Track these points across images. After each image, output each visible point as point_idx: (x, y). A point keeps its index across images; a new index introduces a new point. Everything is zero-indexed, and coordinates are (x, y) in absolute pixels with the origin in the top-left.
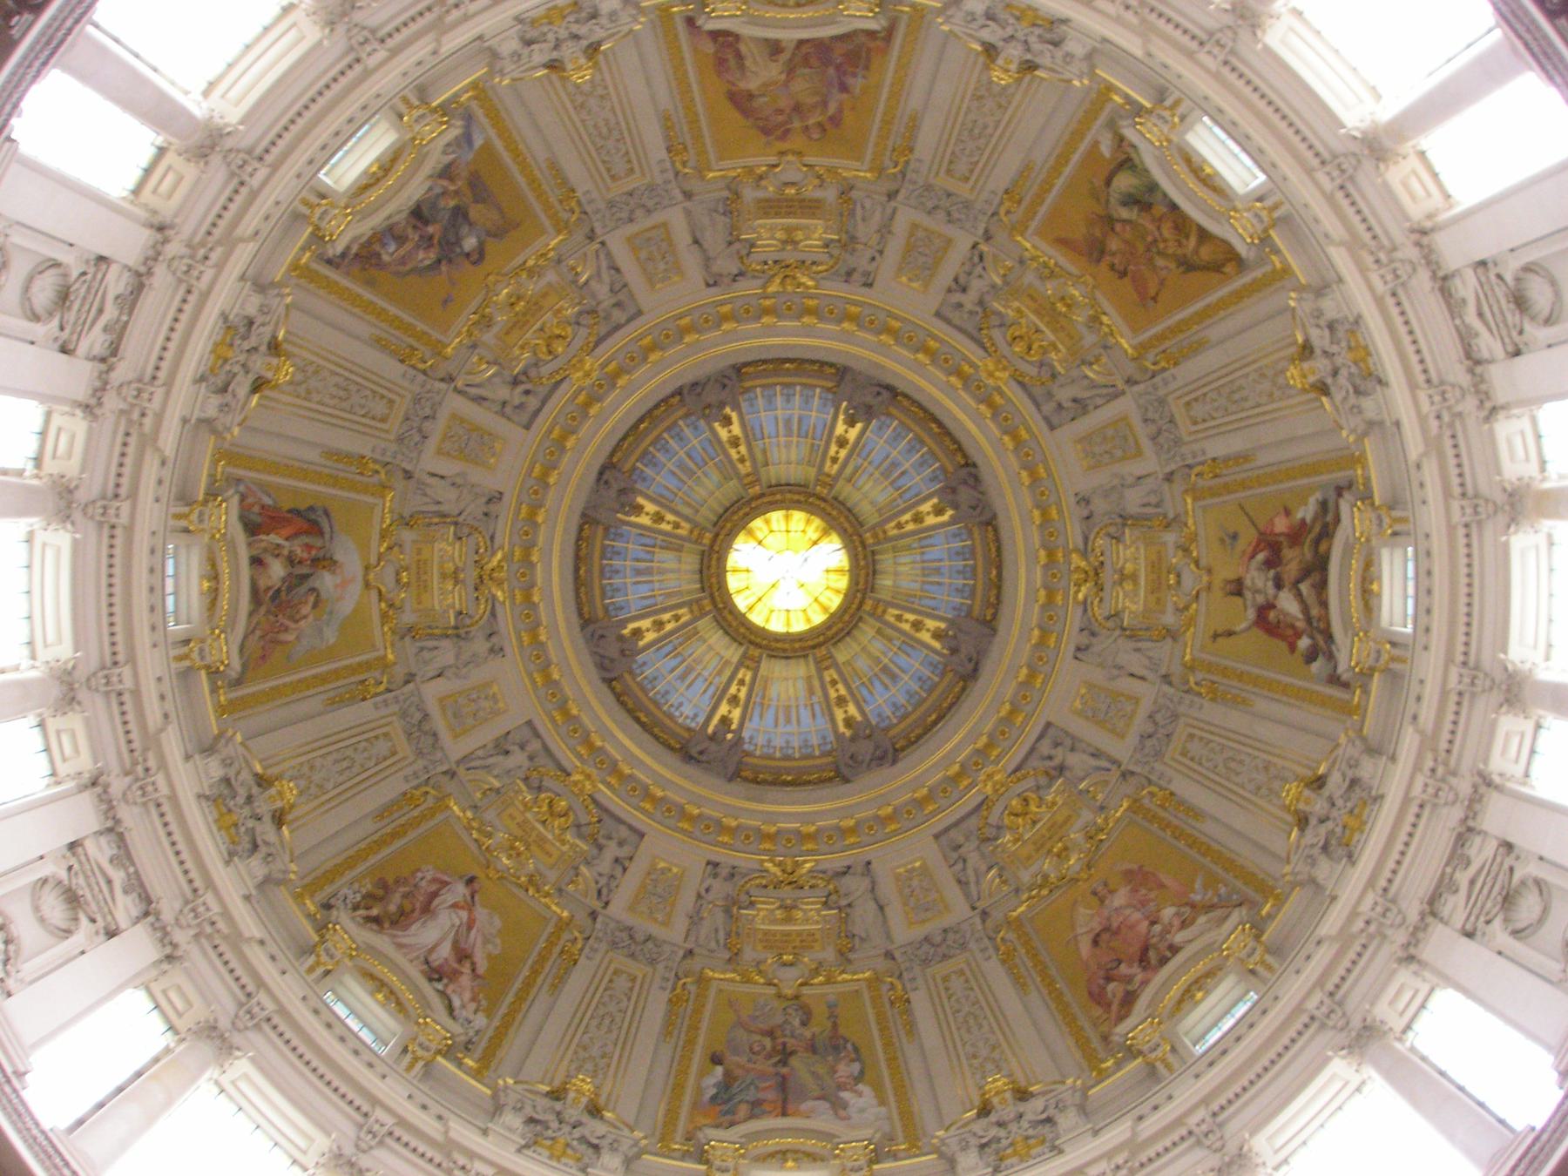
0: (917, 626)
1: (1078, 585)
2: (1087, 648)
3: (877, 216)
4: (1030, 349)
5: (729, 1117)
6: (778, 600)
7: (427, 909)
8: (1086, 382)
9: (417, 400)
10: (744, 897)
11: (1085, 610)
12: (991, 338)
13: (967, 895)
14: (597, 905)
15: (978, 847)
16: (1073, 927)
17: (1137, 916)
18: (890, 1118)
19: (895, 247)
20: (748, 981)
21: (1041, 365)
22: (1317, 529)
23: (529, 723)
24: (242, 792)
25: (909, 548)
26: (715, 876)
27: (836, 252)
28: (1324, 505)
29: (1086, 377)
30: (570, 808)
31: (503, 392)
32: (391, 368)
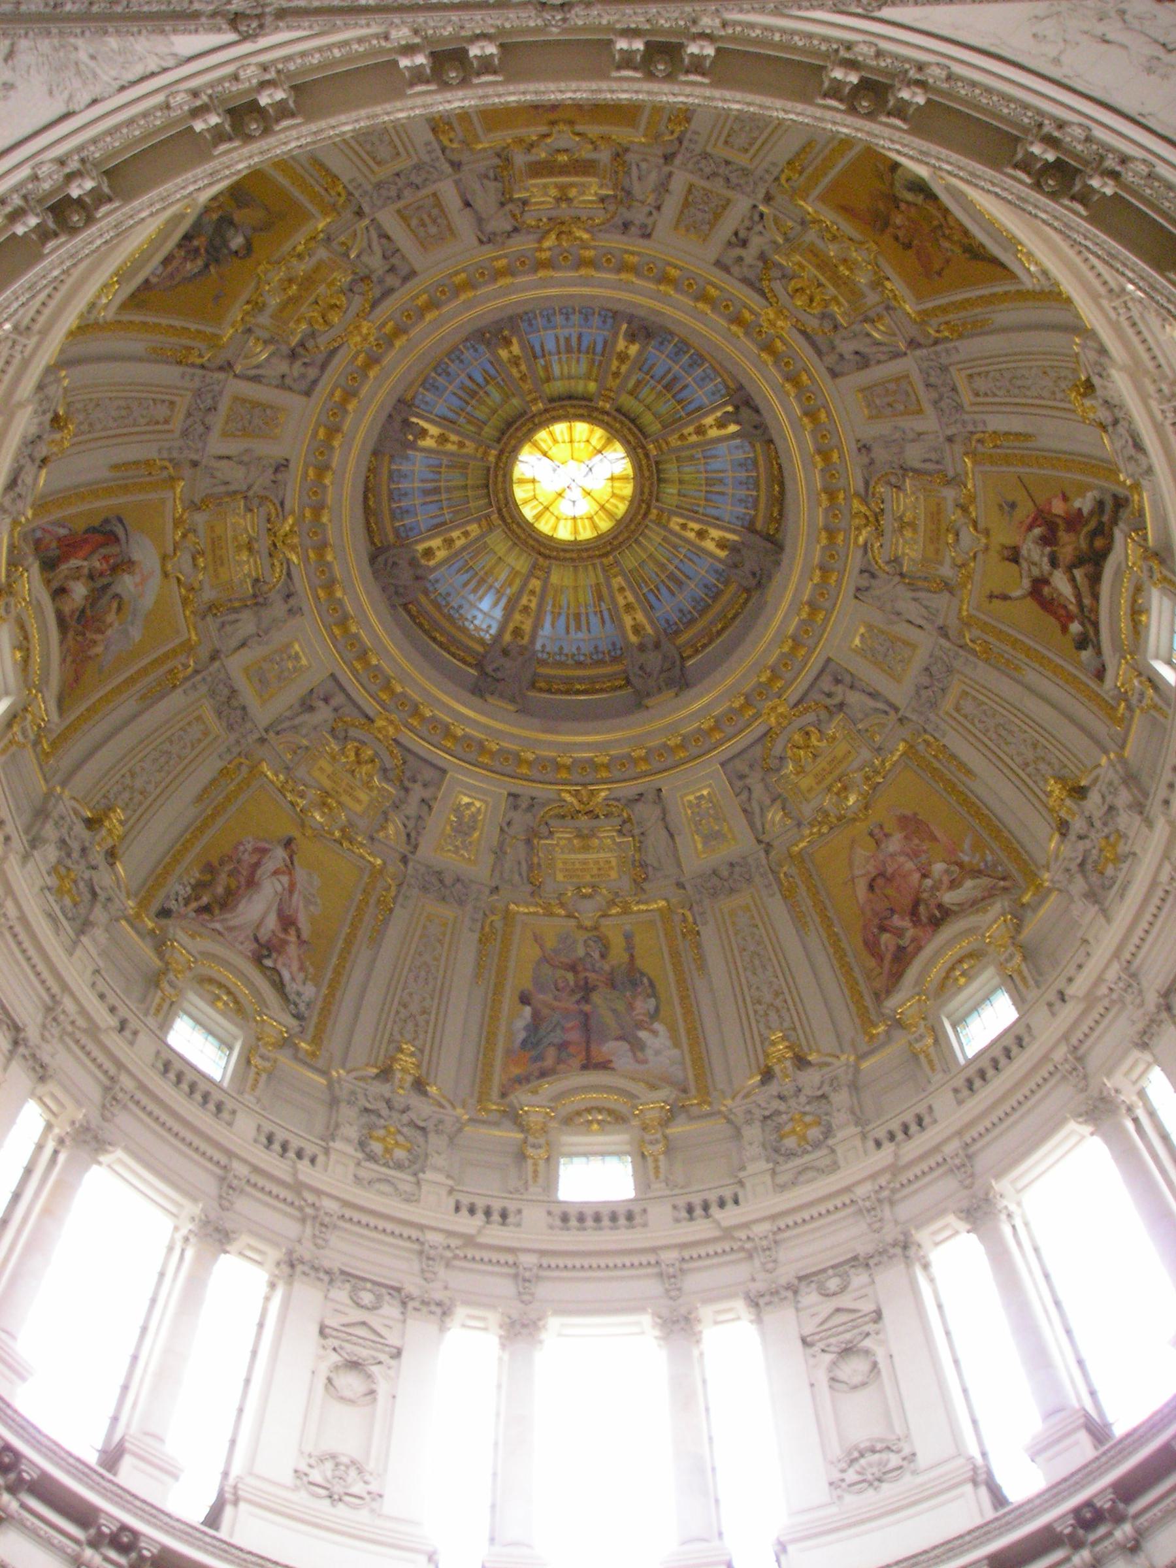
0: (701, 534)
1: (858, 529)
2: (867, 589)
3: (654, 176)
4: (811, 300)
5: (539, 1064)
6: (564, 508)
7: (252, 883)
8: (868, 341)
9: (198, 394)
10: (544, 830)
11: (866, 552)
12: (772, 290)
13: (752, 825)
14: (404, 849)
15: (763, 779)
16: (851, 865)
17: (910, 865)
18: (683, 1063)
19: (672, 205)
20: (551, 914)
21: (823, 316)
22: (1093, 524)
23: (332, 675)
24: (75, 846)
25: (692, 458)
26: (516, 808)
27: (612, 208)
28: (1101, 504)
29: (868, 335)
30: (376, 754)
31: (283, 367)
32: (168, 374)
